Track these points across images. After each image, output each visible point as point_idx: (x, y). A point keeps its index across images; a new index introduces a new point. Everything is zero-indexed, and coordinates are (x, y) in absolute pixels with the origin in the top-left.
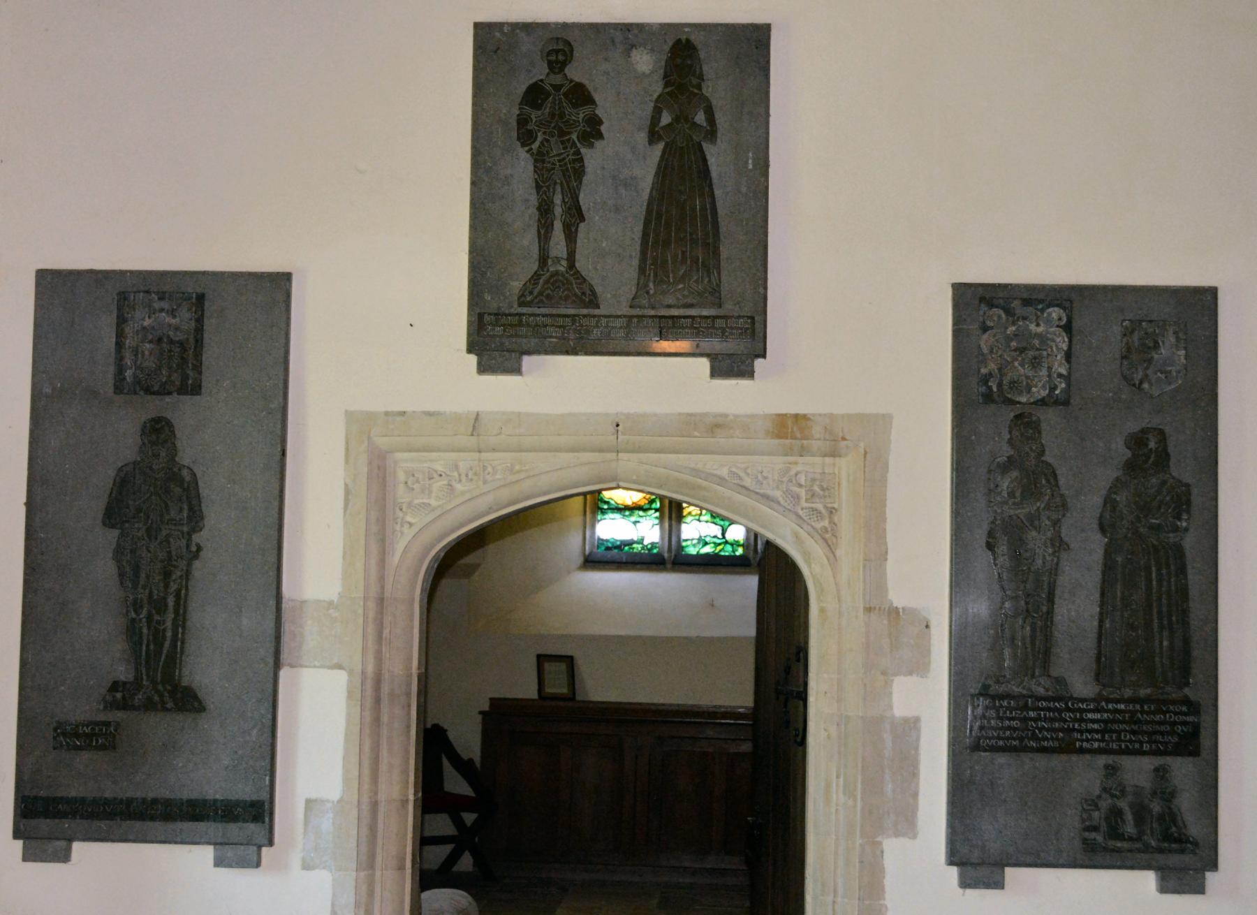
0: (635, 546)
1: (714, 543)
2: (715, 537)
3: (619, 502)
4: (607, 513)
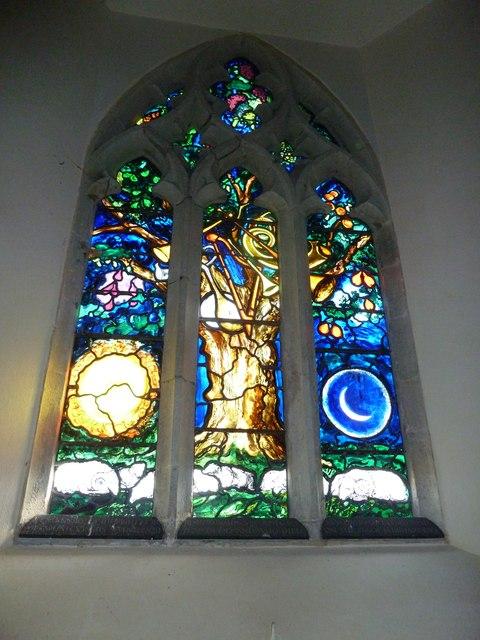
1: (243, 500)
2: (244, 489)
3: (96, 433)
4: (72, 451)
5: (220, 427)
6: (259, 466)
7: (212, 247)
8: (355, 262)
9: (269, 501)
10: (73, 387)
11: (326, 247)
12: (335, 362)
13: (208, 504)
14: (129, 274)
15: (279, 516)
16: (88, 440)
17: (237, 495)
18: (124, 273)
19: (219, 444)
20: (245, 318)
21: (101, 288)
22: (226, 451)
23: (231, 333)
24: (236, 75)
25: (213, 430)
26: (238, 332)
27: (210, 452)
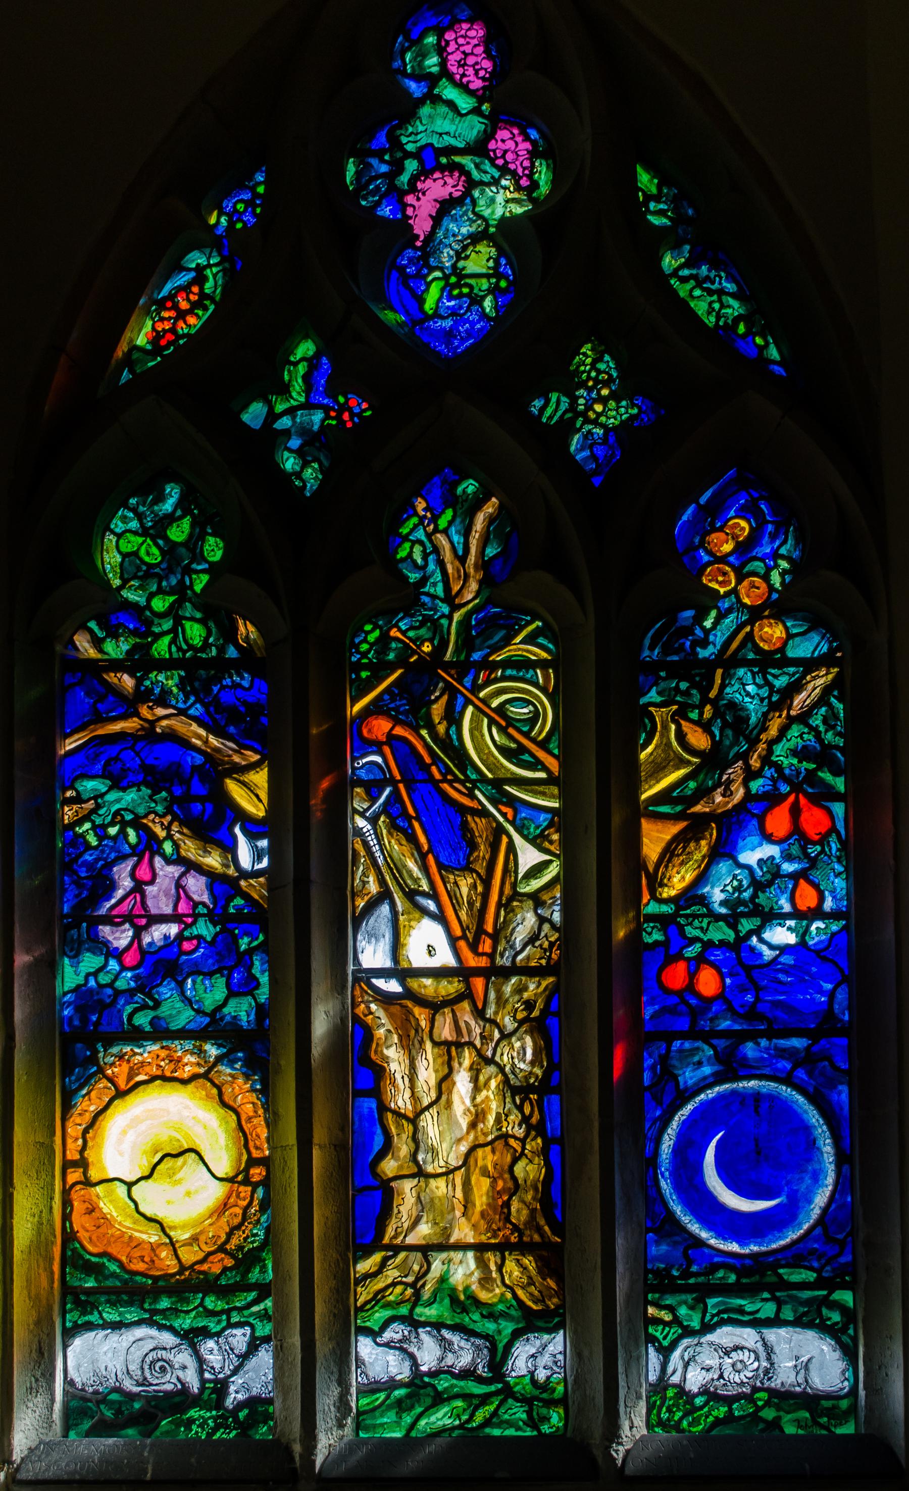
0: (193, 1413)
2: (467, 1374)
4: (94, 1306)
5: (410, 1240)
6: (503, 1323)
7: (378, 759)
8: (778, 767)
9: (527, 1401)
10: (75, 1164)
11: (697, 723)
12: (700, 1064)
13: (390, 1408)
14: (168, 861)
15: (545, 1429)
16: (125, 1282)
17: (453, 1386)
18: (158, 861)
19: (410, 1279)
20: (472, 961)
21: (103, 911)
22: (426, 1294)
23: (435, 1006)
24: (432, 80)
25: (396, 1249)
26: (451, 1002)
27: (391, 1298)
